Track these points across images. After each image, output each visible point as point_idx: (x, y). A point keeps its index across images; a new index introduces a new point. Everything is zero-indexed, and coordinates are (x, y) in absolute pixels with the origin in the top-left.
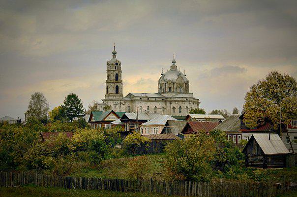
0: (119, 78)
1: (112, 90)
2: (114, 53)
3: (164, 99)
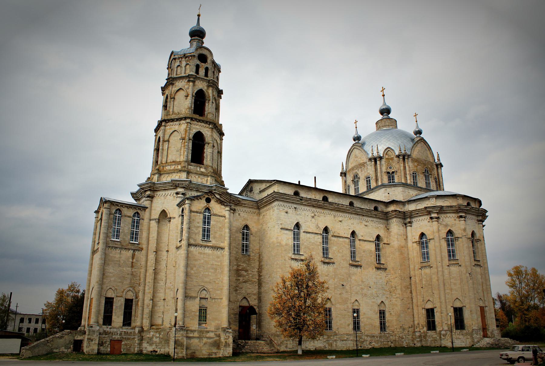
0: (209, 108)
1: (178, 151)
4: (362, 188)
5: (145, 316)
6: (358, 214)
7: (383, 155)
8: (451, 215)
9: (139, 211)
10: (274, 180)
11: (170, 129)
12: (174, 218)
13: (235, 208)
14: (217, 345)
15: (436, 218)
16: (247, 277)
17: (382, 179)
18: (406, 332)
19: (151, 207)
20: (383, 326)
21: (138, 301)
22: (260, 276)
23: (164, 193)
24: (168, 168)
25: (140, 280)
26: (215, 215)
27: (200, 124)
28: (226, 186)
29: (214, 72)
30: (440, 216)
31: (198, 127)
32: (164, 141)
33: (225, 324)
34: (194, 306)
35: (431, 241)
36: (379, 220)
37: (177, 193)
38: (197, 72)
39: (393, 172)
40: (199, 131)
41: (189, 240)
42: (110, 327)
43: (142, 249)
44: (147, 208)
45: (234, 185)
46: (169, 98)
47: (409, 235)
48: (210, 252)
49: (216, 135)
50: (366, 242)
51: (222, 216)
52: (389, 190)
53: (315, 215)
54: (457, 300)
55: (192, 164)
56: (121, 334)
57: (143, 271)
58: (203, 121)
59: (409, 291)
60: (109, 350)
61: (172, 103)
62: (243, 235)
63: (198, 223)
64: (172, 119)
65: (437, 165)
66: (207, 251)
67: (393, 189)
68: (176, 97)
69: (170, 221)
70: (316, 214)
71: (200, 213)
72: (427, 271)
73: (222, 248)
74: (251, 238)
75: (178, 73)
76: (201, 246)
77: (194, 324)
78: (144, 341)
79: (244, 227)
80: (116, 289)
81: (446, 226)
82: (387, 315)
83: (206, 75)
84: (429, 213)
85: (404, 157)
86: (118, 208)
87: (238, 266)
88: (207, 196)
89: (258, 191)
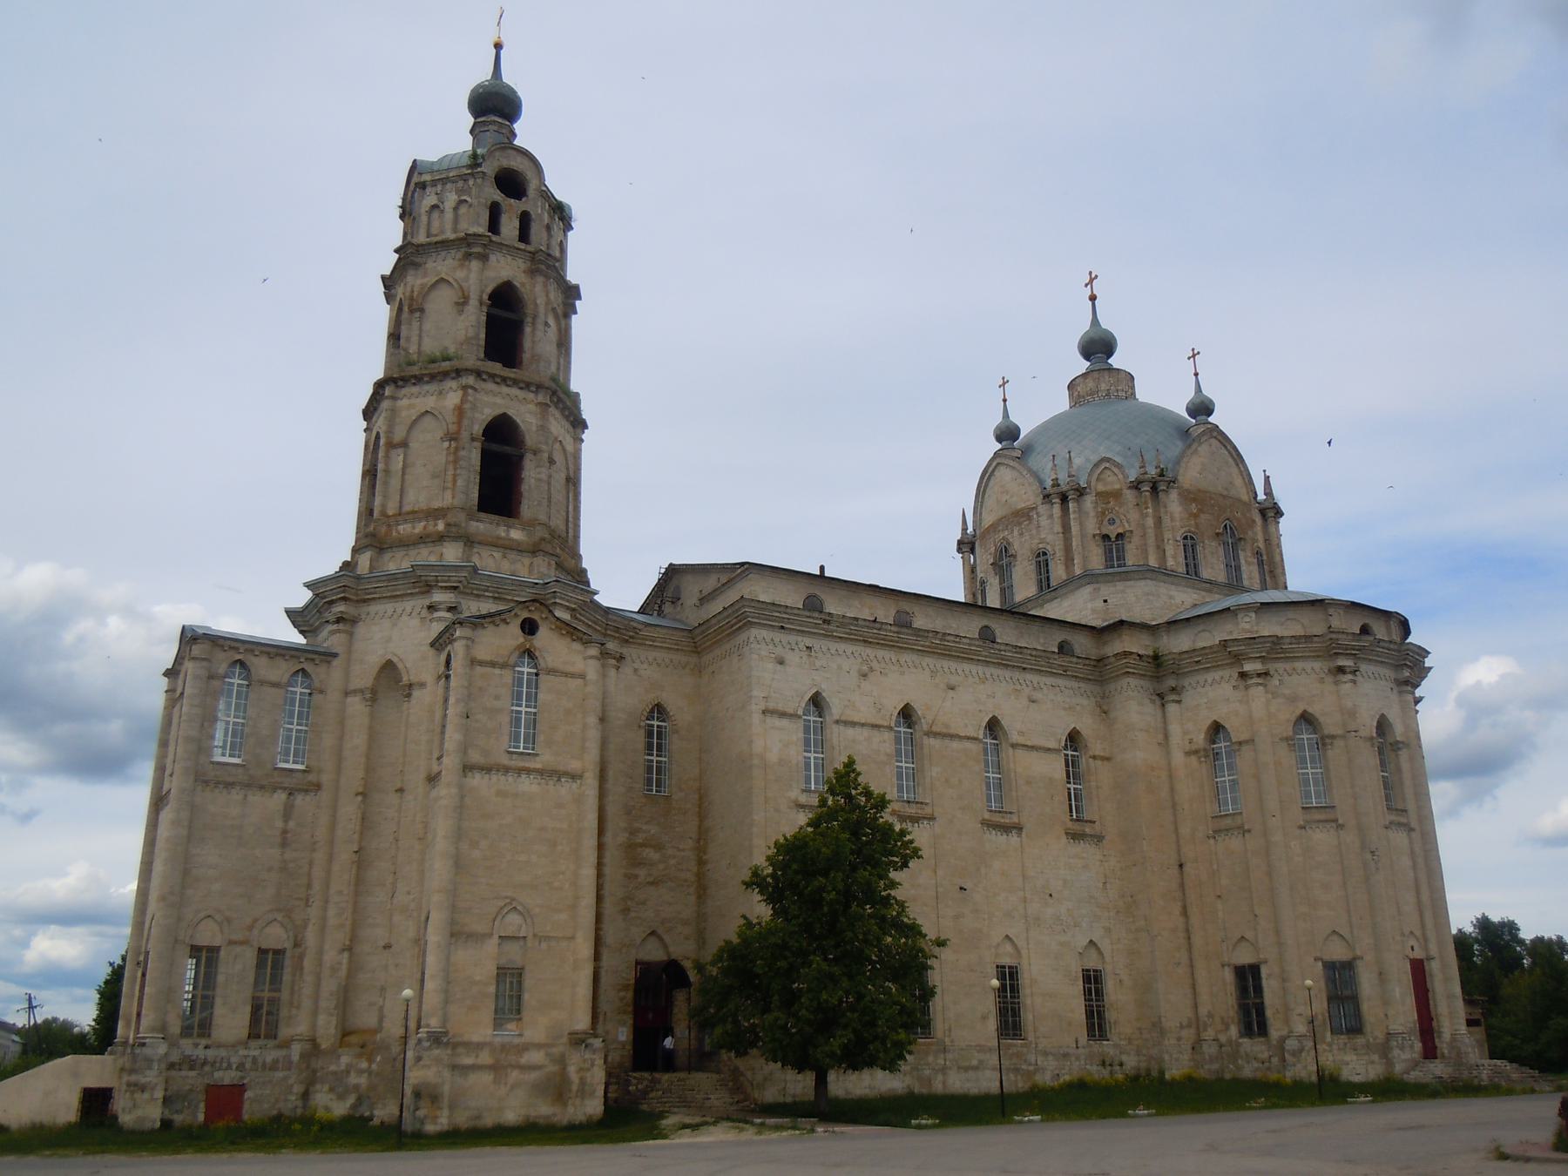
0: (537, 340)
1: (440, 478)
2: (494, 106)
3: (1082, 644)
4: (1024, 588)
5: (323, 1004)
6: (1007, 666)
7: (1089, 482)
8: (1308, 665)
9: (309, 668)
10: (742, 564)
11: (410, 406)
12: (422, 685)
13: (625, 651)
14: (558, 1089)
15: (1259, 675)
16: (661, 866)
17: (1085, 559)
18: (1173, 1041)
19: (349, 652)
20: (1096, 1022)
21: (301, 957)
22: (701, 862)
23: (389, 607)
24: (404, 529)
25: (309, 886)
26: (551, 671)
27: (505, 390)
28: (593, 586)
29: (548, 228)
30: (1271, 667)
31: (499, 400)
32: (391, 445)
33: (582, 1022)
34: (480, 963)
35: (1244, 748)
36: (1075, 684)
37: (432, 608)
38: (494, 226)
39: (1120, 536)
40: (505, 414)
41: (465, 752)
42: (204, 1042)
43: (318, 787)
44: (335, 655)
45: (621, 583)
46: (406, 309)
47: (1175, 729)
48: (535, 788)
49: (558, 426)
50: (1034, 754)
51: (572, 676)
52: (1105, 590)
53: (871, 669)
54: (1335, 938)
55: (483, 515)
56: (241, 1067)
57: (320, 856)
58: (516, 383)
59: (1176, 909)
60: (201, 1117)
61: (415, 325)
62: (650, 734)
63: (497, 698)
64: (415, 377)
65: (1263, 512)
66: (527, 785)
67: (1120, 586)
68: (429, 307)
69: (409, 695)
70: (875, 664)
71: (504, 666)
72: (1235, 843)
73: (574, 777)
74: (675, 743)
75: (434, 231)
76: (506, 770)
77: (479, 1027)
78: (318, 1087)
79: (652, 711)
80: (229, 920)
81: (1293, 699)
82: (1109, 986)
83: (524, 236)
84: (1237, 659)
85: (1155, 486)
86: (238, 657)
87: (633, 832)
88: (525, 615)
89: (695, 600)
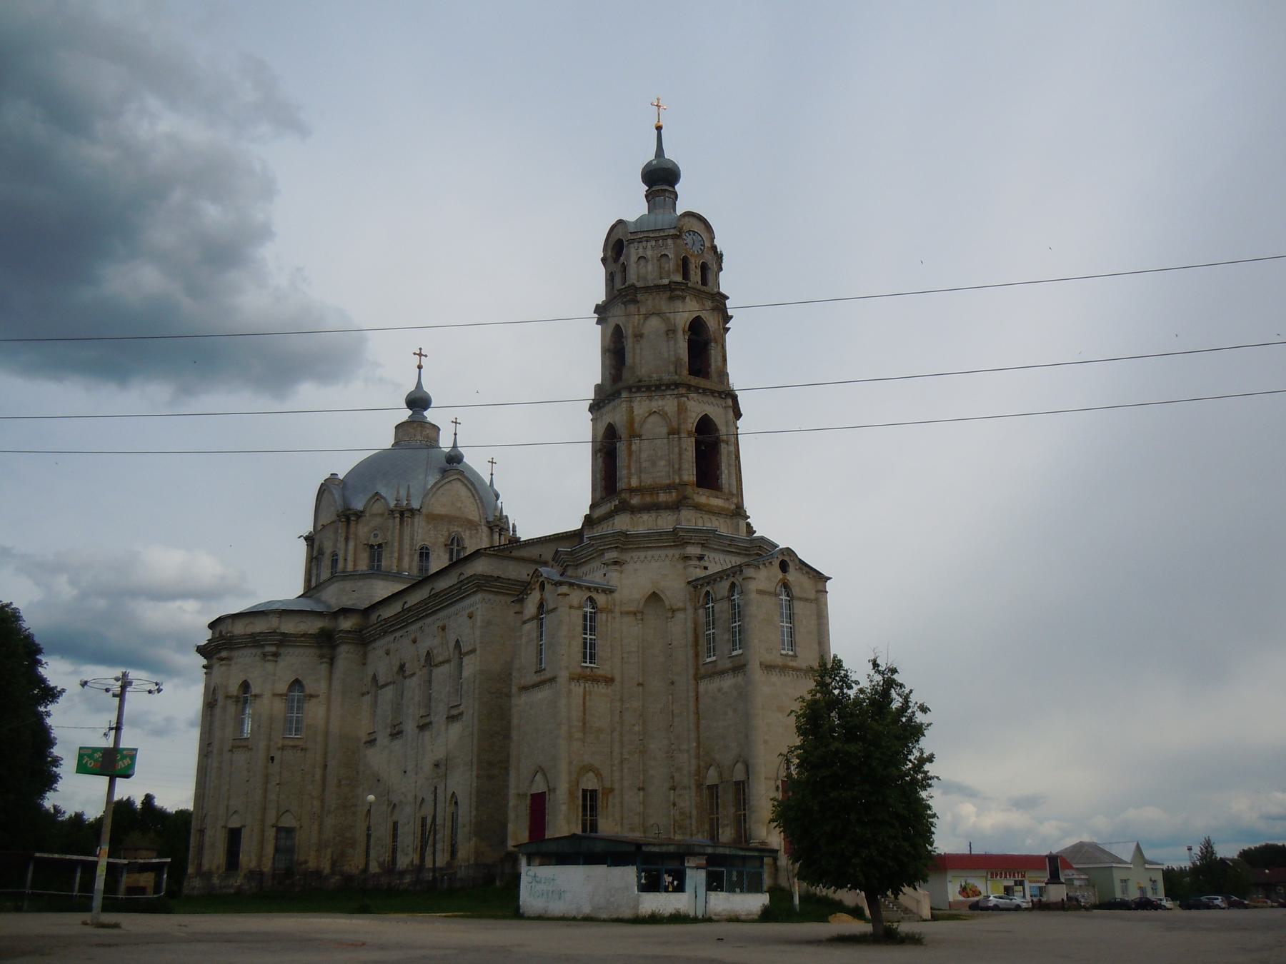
2: (660, 179)
38: (686, 275)
58: (705, 391)
